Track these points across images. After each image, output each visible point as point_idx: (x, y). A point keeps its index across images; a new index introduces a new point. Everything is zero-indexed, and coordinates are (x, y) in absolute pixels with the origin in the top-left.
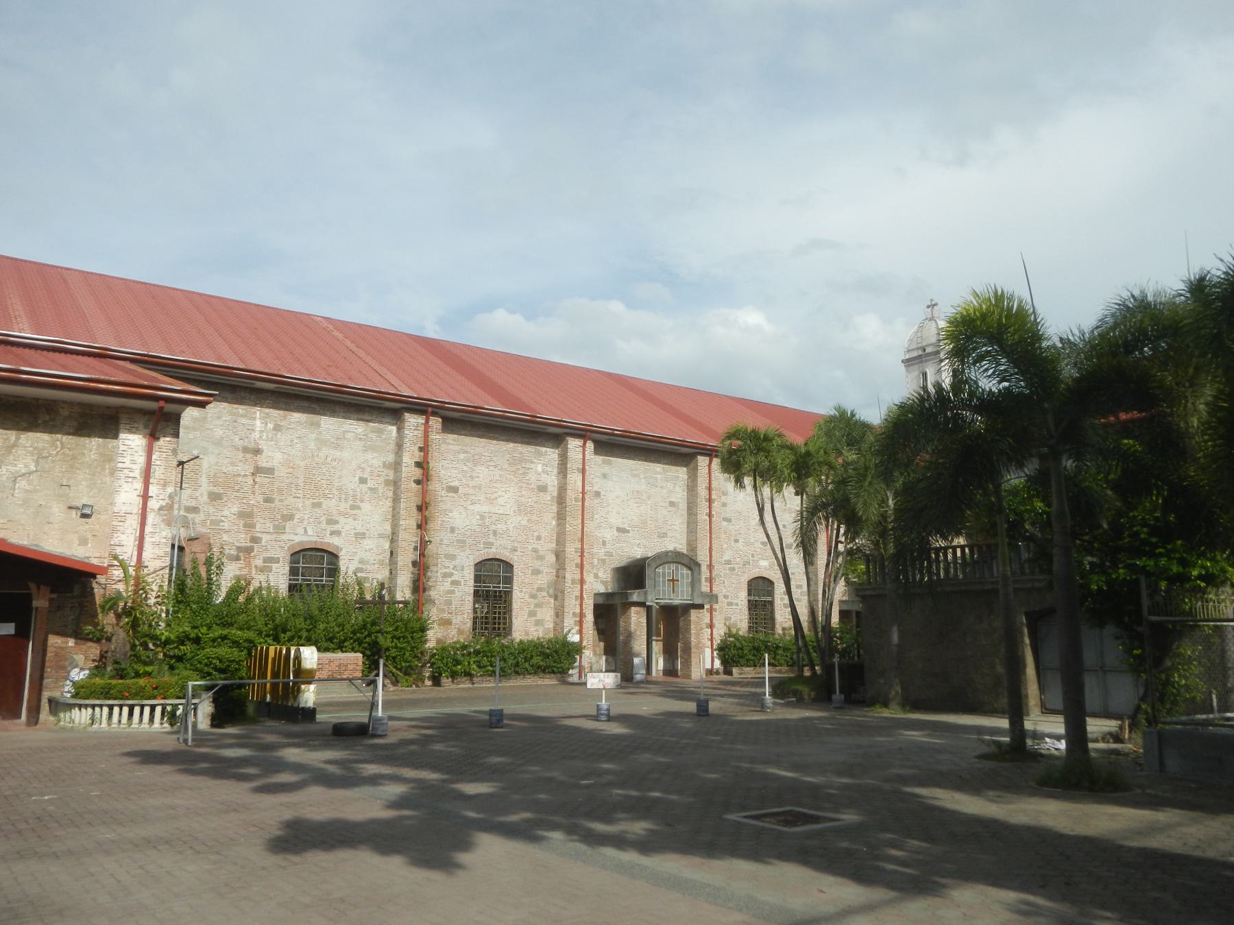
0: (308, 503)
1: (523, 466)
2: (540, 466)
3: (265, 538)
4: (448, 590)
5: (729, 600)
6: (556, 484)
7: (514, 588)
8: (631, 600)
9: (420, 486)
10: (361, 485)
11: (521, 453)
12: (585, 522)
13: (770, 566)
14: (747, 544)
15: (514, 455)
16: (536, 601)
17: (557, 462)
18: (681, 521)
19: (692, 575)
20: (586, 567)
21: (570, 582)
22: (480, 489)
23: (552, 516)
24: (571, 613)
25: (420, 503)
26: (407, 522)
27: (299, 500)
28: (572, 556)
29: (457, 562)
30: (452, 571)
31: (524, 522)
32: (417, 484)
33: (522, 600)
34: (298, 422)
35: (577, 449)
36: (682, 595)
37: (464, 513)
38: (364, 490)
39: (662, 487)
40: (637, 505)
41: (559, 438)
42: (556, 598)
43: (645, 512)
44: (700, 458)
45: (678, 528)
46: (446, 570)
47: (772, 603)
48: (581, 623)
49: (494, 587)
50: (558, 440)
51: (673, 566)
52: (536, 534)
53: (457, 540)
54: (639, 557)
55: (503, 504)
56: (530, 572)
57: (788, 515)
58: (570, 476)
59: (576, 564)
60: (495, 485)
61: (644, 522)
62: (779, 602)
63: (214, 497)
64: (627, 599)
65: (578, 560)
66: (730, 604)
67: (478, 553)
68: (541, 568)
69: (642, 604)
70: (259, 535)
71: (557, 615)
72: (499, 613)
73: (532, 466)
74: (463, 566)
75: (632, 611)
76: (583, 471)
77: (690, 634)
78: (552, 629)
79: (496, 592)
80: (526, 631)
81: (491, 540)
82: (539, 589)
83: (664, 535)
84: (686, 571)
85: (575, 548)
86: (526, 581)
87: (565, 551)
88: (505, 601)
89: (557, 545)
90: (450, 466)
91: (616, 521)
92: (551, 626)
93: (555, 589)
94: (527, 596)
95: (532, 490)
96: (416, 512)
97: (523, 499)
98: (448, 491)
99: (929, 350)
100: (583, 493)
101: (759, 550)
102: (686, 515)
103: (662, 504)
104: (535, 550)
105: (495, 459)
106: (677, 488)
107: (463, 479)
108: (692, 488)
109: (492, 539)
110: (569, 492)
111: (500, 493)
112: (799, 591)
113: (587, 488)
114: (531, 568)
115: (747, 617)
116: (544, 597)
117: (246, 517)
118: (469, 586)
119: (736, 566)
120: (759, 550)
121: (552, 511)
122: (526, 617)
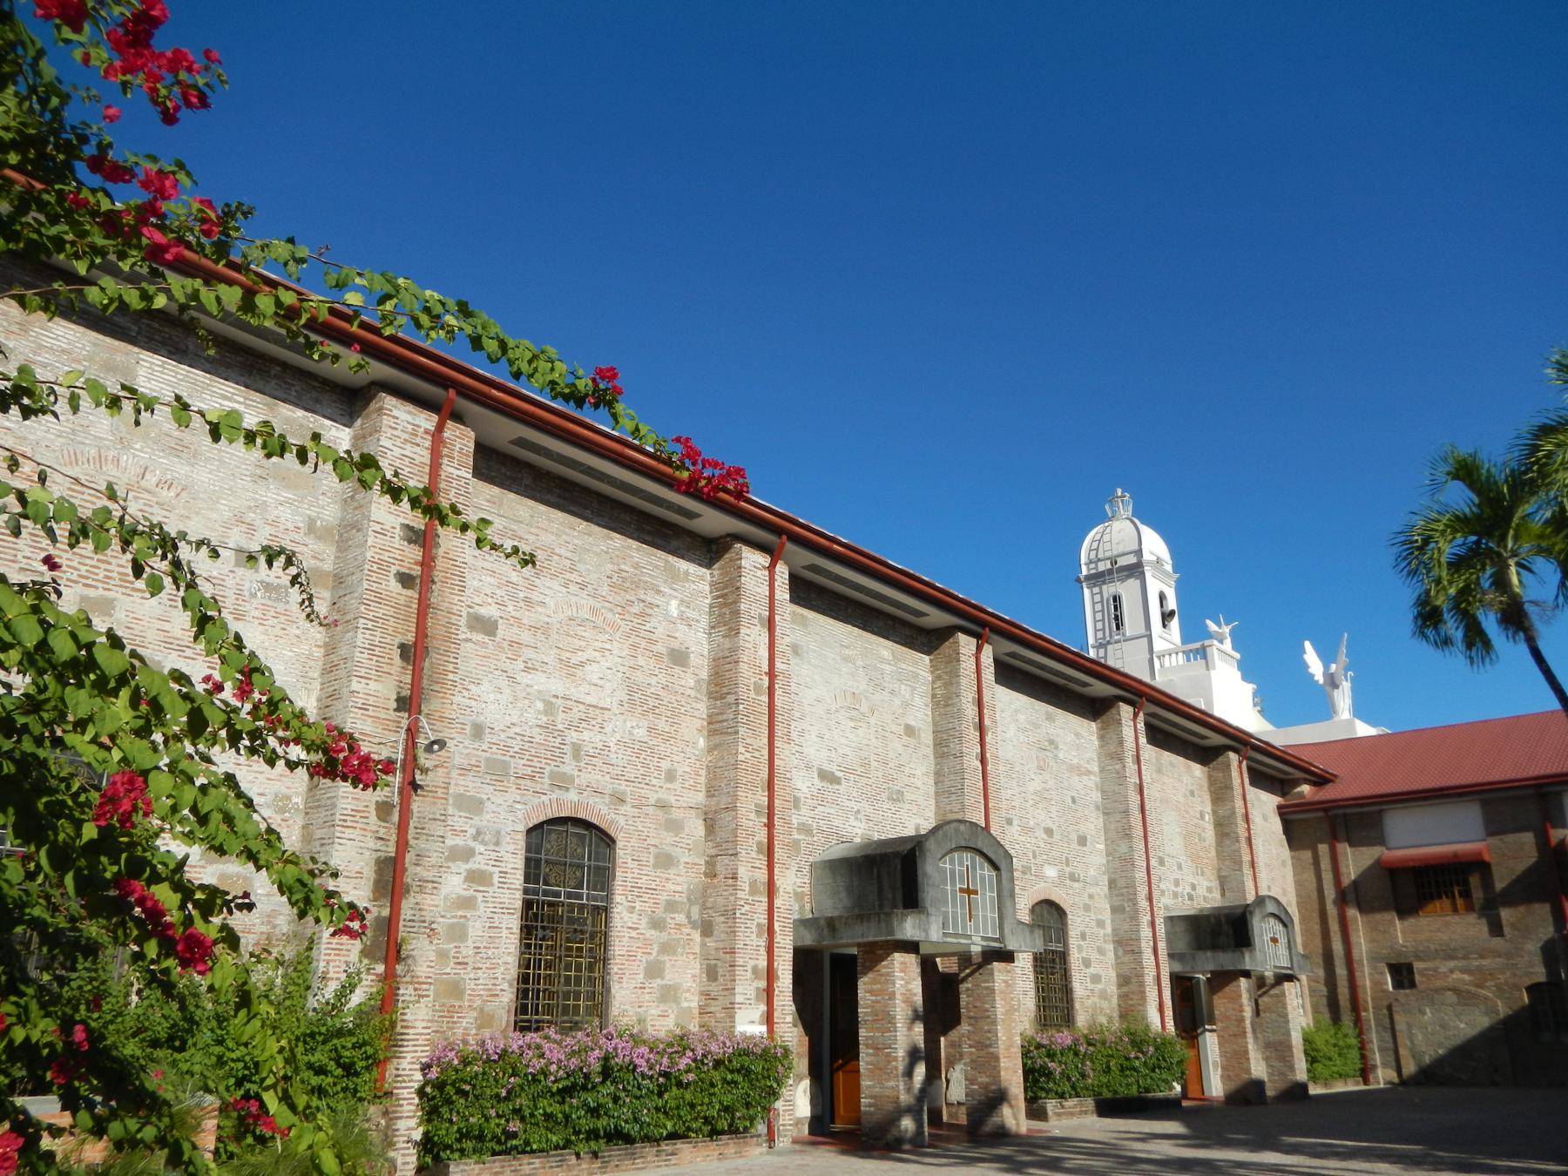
1: (642, 597)
2: (674, 604)
4: (459, 897)
6: (706, 653)
7: (617, 898)
8: (899, 936)
9: (409, 593)
10: (241, 571)
11: (637, 566)
12: (777, 744)
14: (1026, 829)
15: (623, 567)
16: (664, 936)
17: (708, 601)
18: (924, 769)
19: (999, 877)
20: (779, 853)
21: (747, 889)
22: (546, 633)
23: (698, 726)
24: (749, 968)
25: (410, 638)
26: (373, 685)
28: (751, 824)
29: (484, 820)
30: (472, 844)
31: (641, 733)
32: (404, 587)
33: (634, 934)
34: (64, 351)
35: (759, 573)
36: (985, 930)
37: (507, 690)
38: (247, 585)
39: (892, 692)
40: (852, 724)
41: (714, 547)
42: (707, 929)
43: (865, 742)
44: (962, 638)
45: (919, 784)
46: (459, 841)
47: (1063, 956)
48: (769, 993)
49: (569, 895)
50: (709, 551)
51: (967, 857)
52: (665, 765)
53: (487, 759)
54: (858, 840)
55: (595, 681)
56: (652, 860)
57: (1077, 778)
58: (748, 631)
59: (759, 844)
60: (580, 631)
61: (866, 764)
62: (1076, 955)
64: (891, 933)
65: (762, 836)
67: (536, 801)
68: (676, 852)
69: (911, 947)
71: (712, 974)
72: (579, 968)
73: (658, 600)
74: (498, 833)
75: (897, 965)
76: (771, 625)
77: (994, 1023)
78: (696, 1012)
79: (571, 907)
80: (638, 1014)
81: (566, 769)
82: (671, 906)
83: (897, 797)
84: (987, 872)
85: (757, 805)
86: (643, 881)
87: (735, 808)
88: (593, 935)
89: (710, 793)
90: (481, 563)
91: (817, 753)
92: (692, 1002)
93: (704, 907)
94: (644, 921)
95: (658, 656)
96: (397, 661)
97: (639, 677)
98: (471, 628)
99: (1122, 562)
100: (772, 674)
101: (1042, 845)
102: (932, 757)
103: (894, 728)
104: (662, 806)
105: (581, 567)
106: (918, 701)
107: (508, 603)
108: (943, 702)
109: (569, 767)
110: (743, 667)
111: (589, 654)
112: (1102, 932)
113: (779, 665)
114: (652, 849)
115: (1033, 985)
116: (679, 926)
118: (509, 892)
120: (1042, 845)
121: (696, 713)
122: (641, 976)
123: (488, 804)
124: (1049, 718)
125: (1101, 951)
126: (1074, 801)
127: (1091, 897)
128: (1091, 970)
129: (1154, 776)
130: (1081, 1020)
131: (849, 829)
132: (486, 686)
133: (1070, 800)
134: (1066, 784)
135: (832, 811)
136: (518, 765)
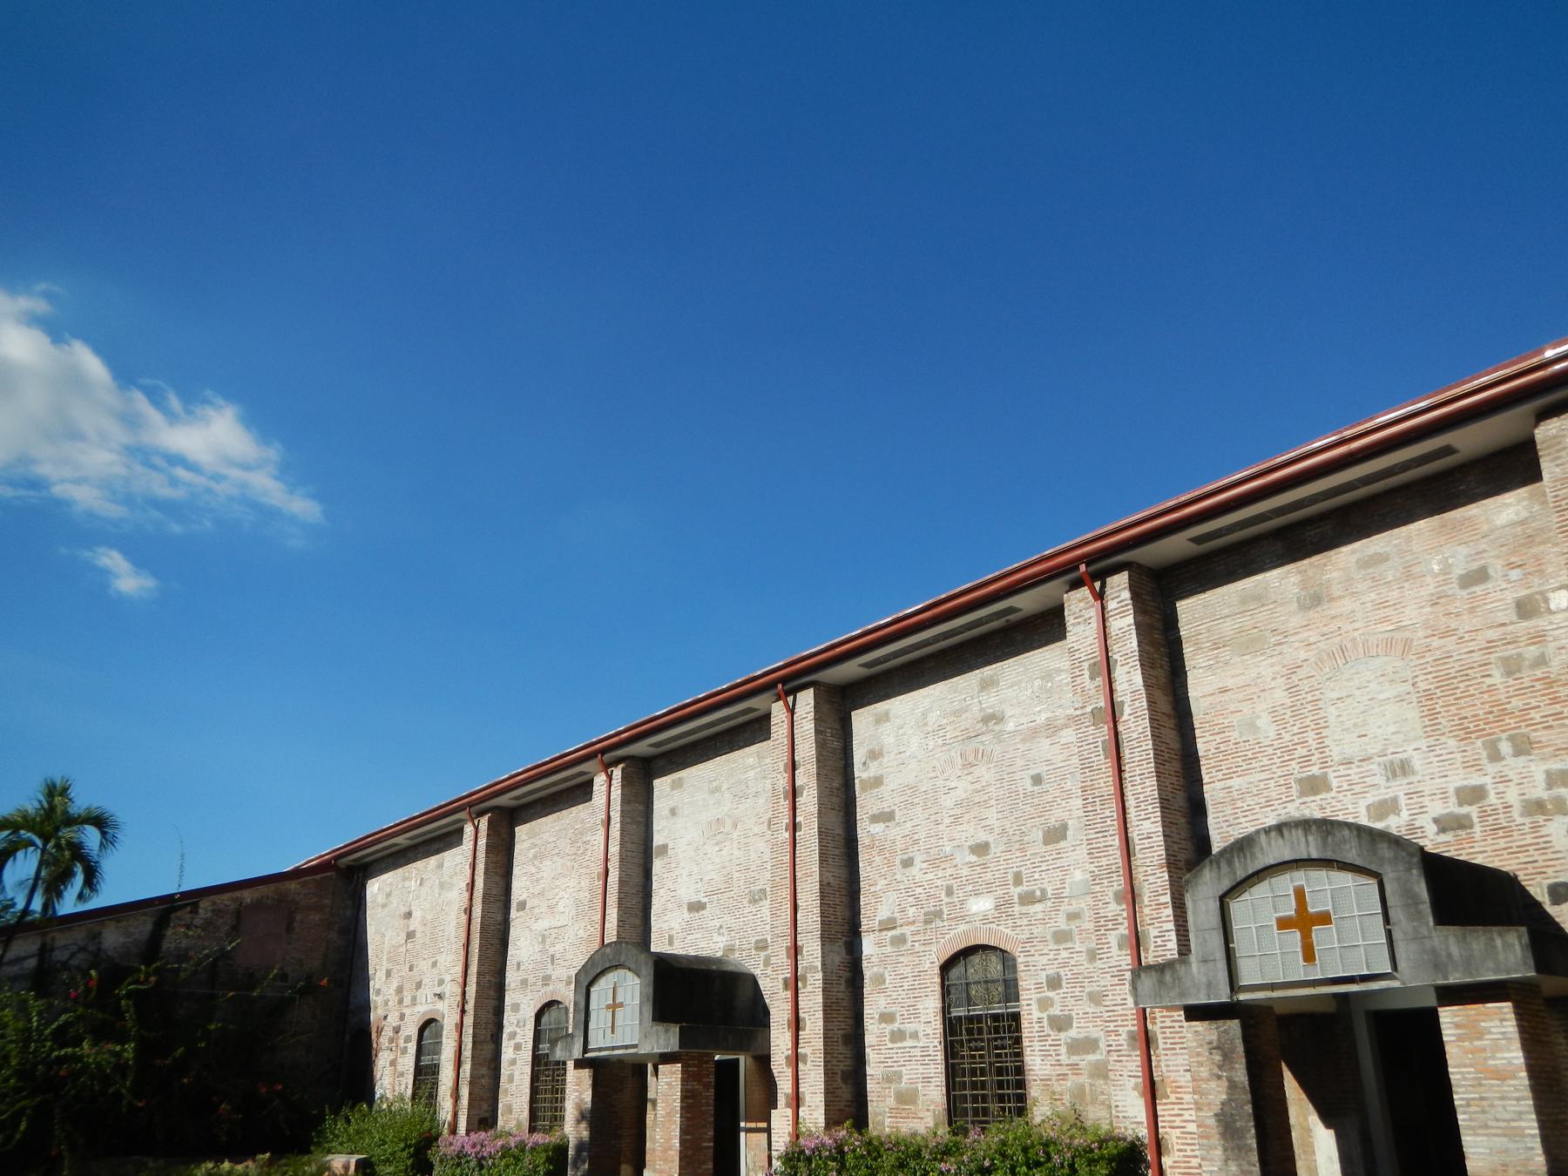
0: (430, 962)
1: (585, 840)
3: (407, 1011)
5: (895, 1026)
13: (997, 907)
27: (425, 962)
57: (1048, 741)
60: (557, 883)
61: (729, 879)
62: (1036, 1014)
63: (388, 974)
66: (898, 1036)
70: (404, 1011)
81: (548, 972)
117: (400, 990)
119: (907, 930)
120: (965, 872)
123: (522, 1006)
124: (985, 685)
125: (1095, 998)
126: (1037, 780)
127: (1073, 916)
128: (1073, 1033)
129: (1296, 621)
130: (1040, 1111)
131: (713, 946)
132: (522, 939)
133: (1028, 782)
134: (1020, 762)
135: (698, 936)
136: (531, 980)
